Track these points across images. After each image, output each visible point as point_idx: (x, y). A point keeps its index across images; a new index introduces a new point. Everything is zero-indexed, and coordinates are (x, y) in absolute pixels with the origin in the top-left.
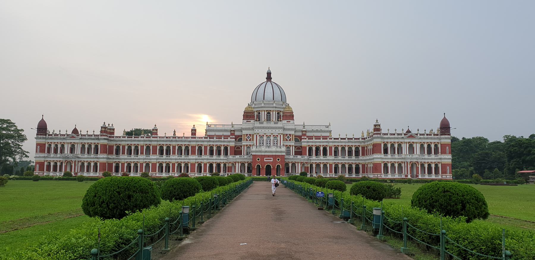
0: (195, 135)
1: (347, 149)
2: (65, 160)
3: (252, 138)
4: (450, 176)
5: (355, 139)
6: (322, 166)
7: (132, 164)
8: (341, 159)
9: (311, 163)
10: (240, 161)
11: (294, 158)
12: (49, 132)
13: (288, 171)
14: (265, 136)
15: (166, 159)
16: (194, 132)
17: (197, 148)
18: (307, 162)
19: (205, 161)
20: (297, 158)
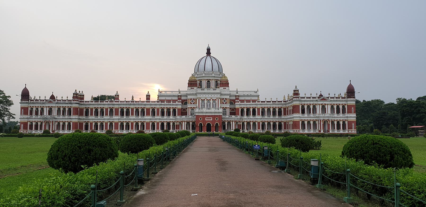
0: (149, 100)
1: (272, 110)
2: (44, 120)
3: (195, 101)
4: (355, 131)
5: (278, 102)
6: (252, 123)
7: (99, 123)
8: (267, 118)
9: (243, 122)
10: (185, 120)
11: (230, 117)
12: (31, 98)
13: (224, 128)
14: (206, 100)
15: (126, 119)
16: (148, 97)
17: (151, 110)
18: (239, 120)
19: (158, 121)
20: (232, 117)
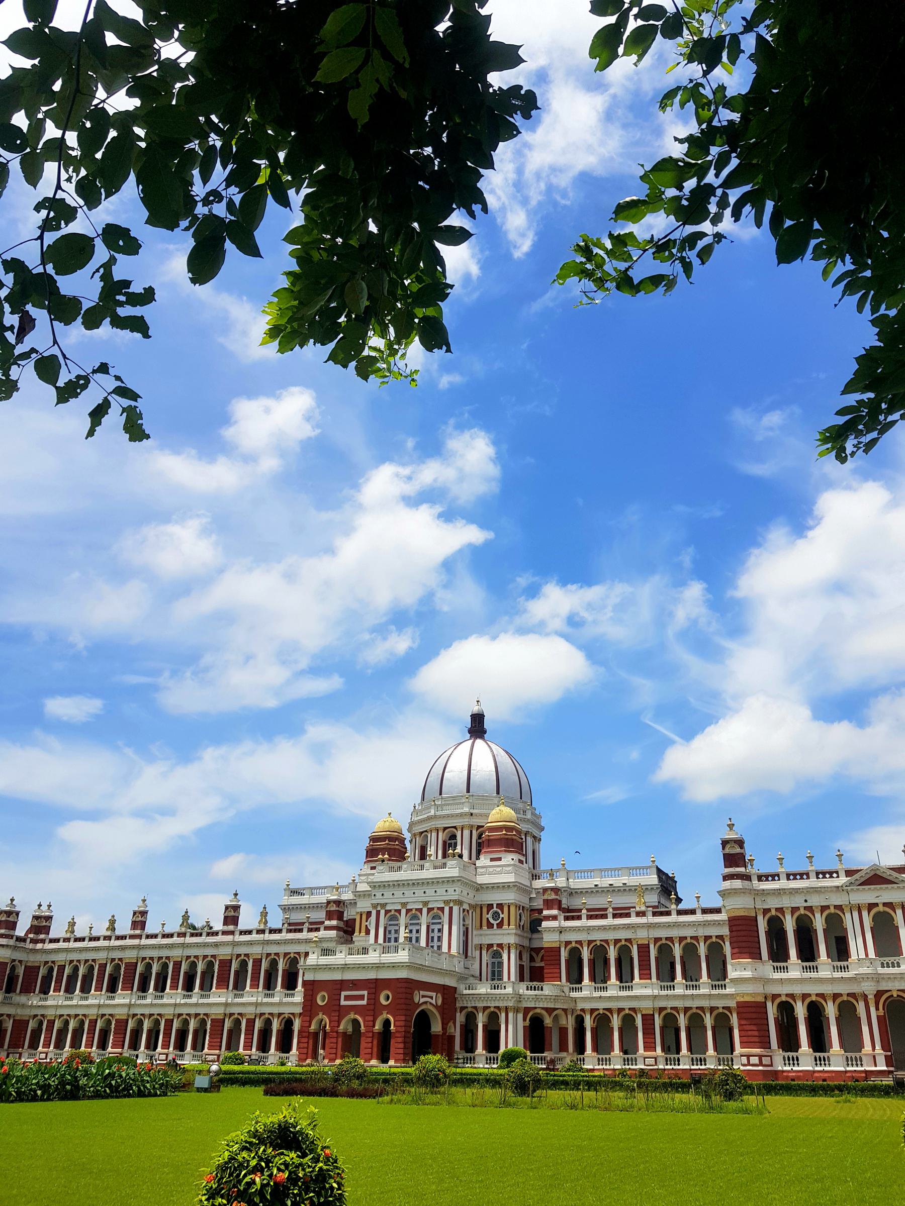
5: (705, 911)
9: (579, 1012)
19: (250, 1011)
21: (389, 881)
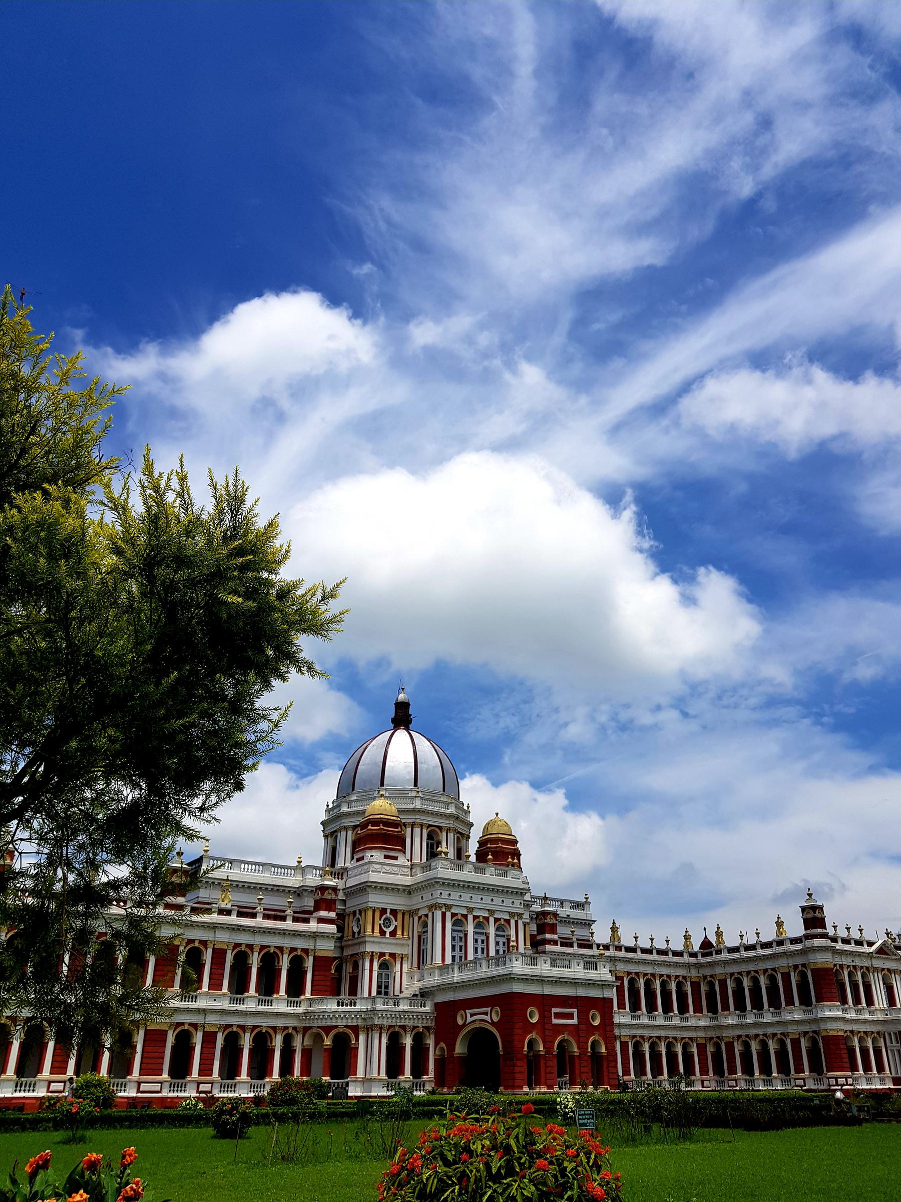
21: (460, 881)
